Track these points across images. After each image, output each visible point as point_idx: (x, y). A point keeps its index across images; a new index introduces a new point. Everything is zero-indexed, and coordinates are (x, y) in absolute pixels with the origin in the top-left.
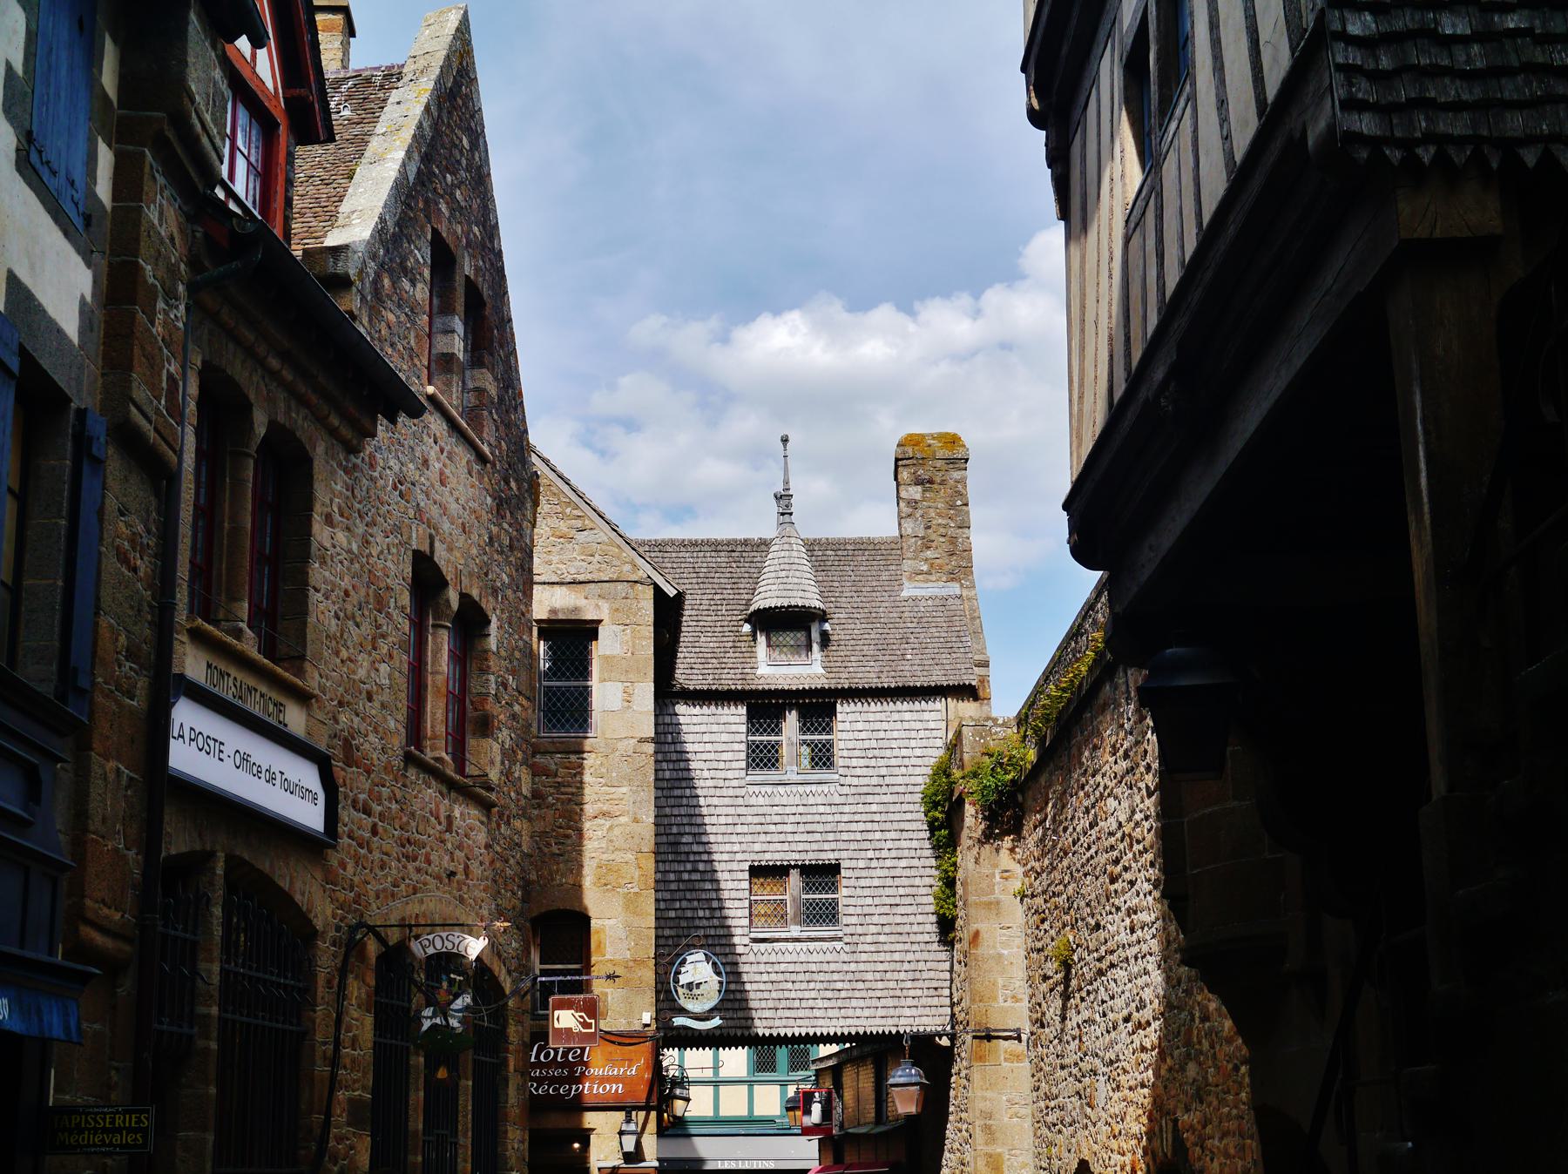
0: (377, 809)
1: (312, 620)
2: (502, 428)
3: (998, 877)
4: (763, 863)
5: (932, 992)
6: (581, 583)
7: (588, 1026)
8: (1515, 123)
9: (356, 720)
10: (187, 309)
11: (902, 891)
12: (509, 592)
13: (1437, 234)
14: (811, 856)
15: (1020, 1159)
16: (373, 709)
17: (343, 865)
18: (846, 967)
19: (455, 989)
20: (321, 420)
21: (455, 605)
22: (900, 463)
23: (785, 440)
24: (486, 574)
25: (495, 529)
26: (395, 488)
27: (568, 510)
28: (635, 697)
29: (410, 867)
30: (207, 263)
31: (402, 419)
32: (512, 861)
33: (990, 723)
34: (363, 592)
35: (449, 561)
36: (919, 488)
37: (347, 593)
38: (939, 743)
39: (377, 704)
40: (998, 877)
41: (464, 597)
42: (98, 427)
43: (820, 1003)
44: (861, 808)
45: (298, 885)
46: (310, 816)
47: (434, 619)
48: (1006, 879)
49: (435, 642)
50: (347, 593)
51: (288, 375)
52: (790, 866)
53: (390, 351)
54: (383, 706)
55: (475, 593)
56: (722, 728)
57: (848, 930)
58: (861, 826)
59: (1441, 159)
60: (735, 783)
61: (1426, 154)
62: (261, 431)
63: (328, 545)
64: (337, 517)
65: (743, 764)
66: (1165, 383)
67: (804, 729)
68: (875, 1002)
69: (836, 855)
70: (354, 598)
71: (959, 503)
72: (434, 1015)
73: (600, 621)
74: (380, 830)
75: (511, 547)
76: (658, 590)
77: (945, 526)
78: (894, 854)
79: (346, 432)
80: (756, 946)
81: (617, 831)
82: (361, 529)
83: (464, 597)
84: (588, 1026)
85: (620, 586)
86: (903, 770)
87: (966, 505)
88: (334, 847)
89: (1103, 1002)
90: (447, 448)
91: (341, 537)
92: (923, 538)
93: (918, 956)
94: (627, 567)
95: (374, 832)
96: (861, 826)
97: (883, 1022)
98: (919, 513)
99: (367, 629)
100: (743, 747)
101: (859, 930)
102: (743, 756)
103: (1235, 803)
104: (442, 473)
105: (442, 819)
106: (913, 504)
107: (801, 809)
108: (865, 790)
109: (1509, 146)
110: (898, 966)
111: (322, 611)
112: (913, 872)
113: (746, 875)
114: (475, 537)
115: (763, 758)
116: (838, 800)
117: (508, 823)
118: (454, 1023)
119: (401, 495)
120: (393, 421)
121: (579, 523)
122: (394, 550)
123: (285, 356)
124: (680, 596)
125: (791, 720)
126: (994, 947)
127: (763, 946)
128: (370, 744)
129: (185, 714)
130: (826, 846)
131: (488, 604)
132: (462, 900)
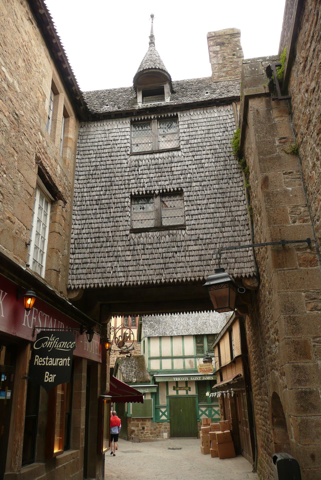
22: (209, 39)
36: (219, 46)
40: (277, 143)
71: (238, 49)
77: (231, 58)
87: (241, 49)
92: (222, 64)
98: (219, 55)
126: (281, 186)
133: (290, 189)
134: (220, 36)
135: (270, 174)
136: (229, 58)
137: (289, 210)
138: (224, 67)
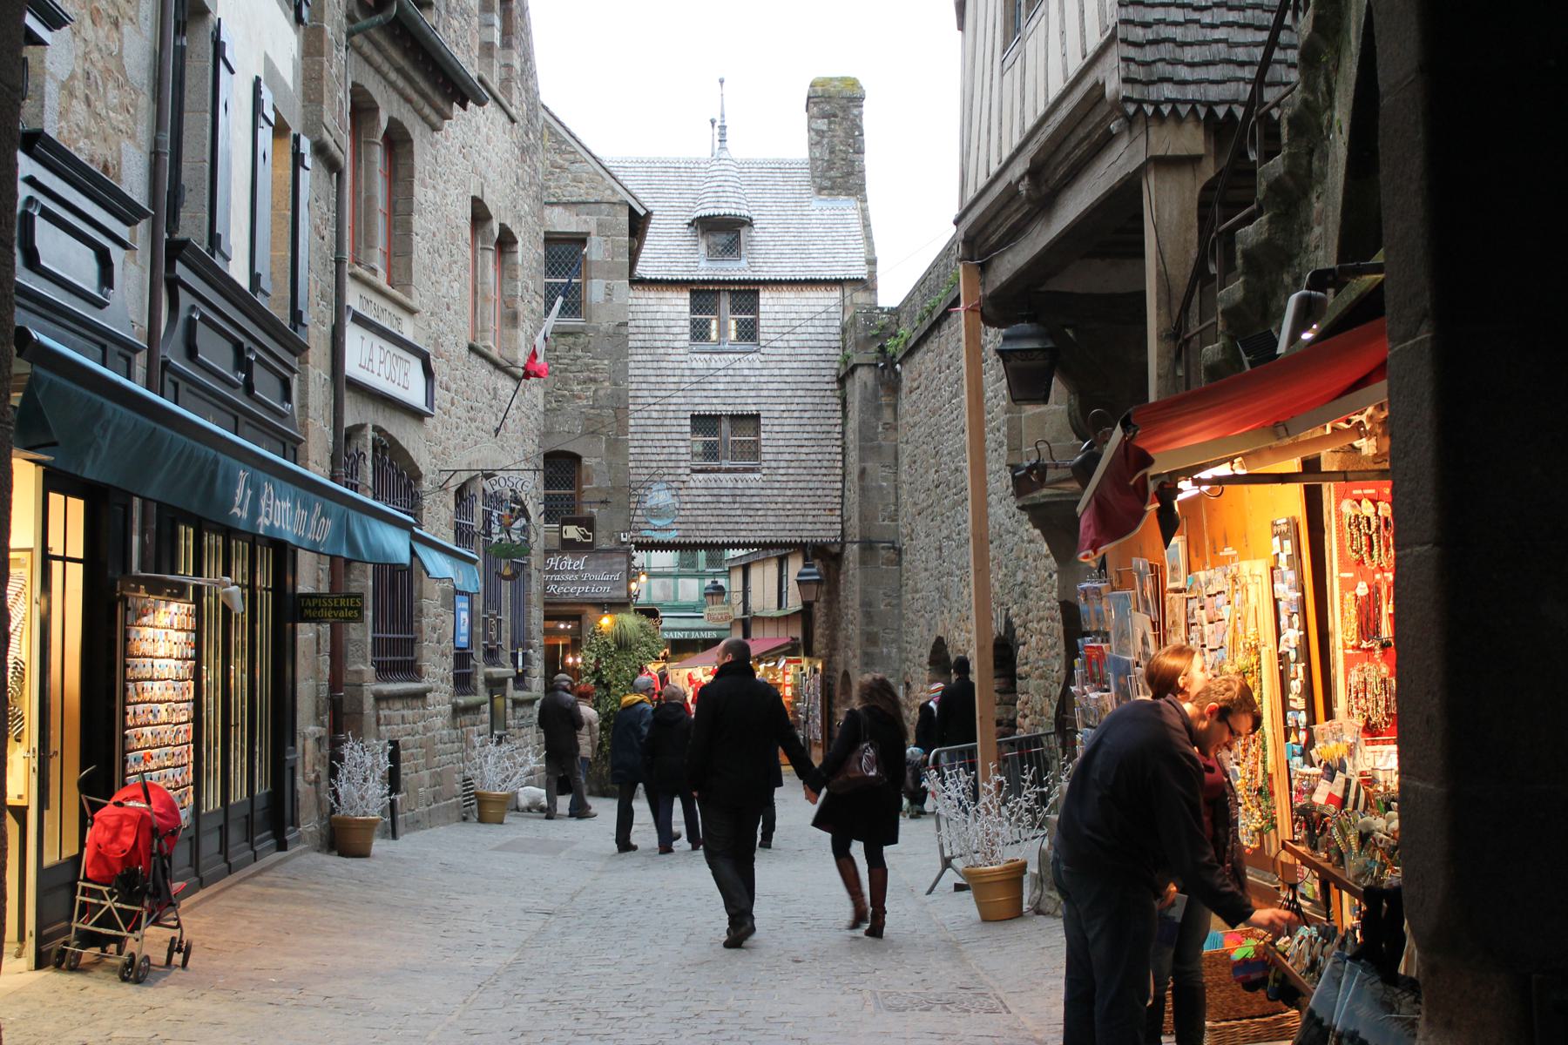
0: (454, 387)
1: (415, 256)
2: (524, 93)
3: (880, 429)
4: (702, 413)
5: (827, 512)
6: (573, 203)
7: (588, 537)
8: (1213, 93)
9: (441, 324)
10: (347, 49)
11: (806, 436)
12: (529, 218)
13: (1169, 153)
14: (740, 408)
15: (892, 636)
16: (450, 316)
17: (435, 428)
18: (762, 492)
19: (515, 514)
20: (419, 112)
21: (497, 234)
22: (811, 100)
23: (722, 81)
24: (515, 207)
25: (520, 171)
26: (460, 152)
27: (563, 147)
28: (615, 291)
29: (473, 425)
30: (358, 16)
31: (470, 104)
32: (532, 418)
33: (878, 311)
34: (443, 232)
35: (492, 201)
36: (826, 121)
37: (434, 235)
38: (838, 323)
39: (453, 312)
40: (880, 429)
41: (502, 226)
42: (306, 145)
43: (744, 519)
44: (776, 372)
45: (411, 443)
46: (414, 394)
47: (482, 243)
48: (887, 429)
49: (483, 261)
50: (434, 235)
51: (401, 83)
52: (721, 415)
53: (455, 49)
54: (456, 313)
55: (508, 223)
56: (672, 309)
57: (764, 464)
58: (775, 386)
59: (1174, 111)
60: (682, 351)
61: (1166, 109)
62: (384, 125)
63: (423, 201)
64: (428, 180)
65: (687, 337)
66: (1022, 178)
67: (734, 310)
68: (783, 519)
69: (757, 408)
70: (439, 236)
71: (857, 133)
72: (501, 532)
73: (588, 234)
74: (456, 401)
75: (530, 184)
76: (632, 211)
78: (801, 407)
79: (434, 118)
80: (695, 476)
81: (601, 393)
82: (441, 187)
83: (502, 226)
84: (588, 537)
85: (603, 207)
86: (810, 344)
87: (862, 135)
88: (432, 416)
89: (959, 525)
90: (491, 116)
91: (430, 193)
92: (828, 161)
93: (817, 485)
94: (609, 192)
95: (453, 404)
96: (775, 386)
97: (790, 534)
98: (825, 141)
99: (446, 258)
100: (688, 323)
101: (774, 464)
102: (687, 330)
103: (1057, 407)
104: (487, 136)
105: (491, 391)
106: (818, 132)
107: (730, 372)
108: (779, 358)
109: (1210, 105)
110: (802, 492)
111: (420, 246)
112: (815, 421)
113: (688, 422)
114: (508, 180)
115: (699, 332)
116: (758, 365)
117: (529, 390)
118: (514, 537)
119: (464, 157)
120: (464, 108)
121: (571, 157)
122: (460, 198)
123: (399, 70)
124: (649, 214)
125: (725, 303)
127: (701, 476)
128: (448, 341)
129: (354, 336)
130: (750, 401)
131: (515, 230)
132: (502, 447)
133: (885, 484)
134: (830, 97)
135: (869, 465)
136: (841, 150)
137: (880, 507)
138: (832, 169)
